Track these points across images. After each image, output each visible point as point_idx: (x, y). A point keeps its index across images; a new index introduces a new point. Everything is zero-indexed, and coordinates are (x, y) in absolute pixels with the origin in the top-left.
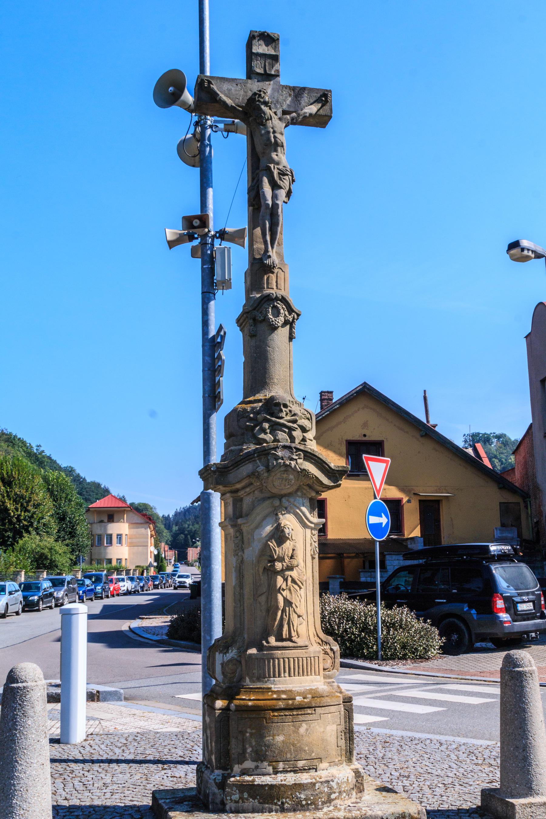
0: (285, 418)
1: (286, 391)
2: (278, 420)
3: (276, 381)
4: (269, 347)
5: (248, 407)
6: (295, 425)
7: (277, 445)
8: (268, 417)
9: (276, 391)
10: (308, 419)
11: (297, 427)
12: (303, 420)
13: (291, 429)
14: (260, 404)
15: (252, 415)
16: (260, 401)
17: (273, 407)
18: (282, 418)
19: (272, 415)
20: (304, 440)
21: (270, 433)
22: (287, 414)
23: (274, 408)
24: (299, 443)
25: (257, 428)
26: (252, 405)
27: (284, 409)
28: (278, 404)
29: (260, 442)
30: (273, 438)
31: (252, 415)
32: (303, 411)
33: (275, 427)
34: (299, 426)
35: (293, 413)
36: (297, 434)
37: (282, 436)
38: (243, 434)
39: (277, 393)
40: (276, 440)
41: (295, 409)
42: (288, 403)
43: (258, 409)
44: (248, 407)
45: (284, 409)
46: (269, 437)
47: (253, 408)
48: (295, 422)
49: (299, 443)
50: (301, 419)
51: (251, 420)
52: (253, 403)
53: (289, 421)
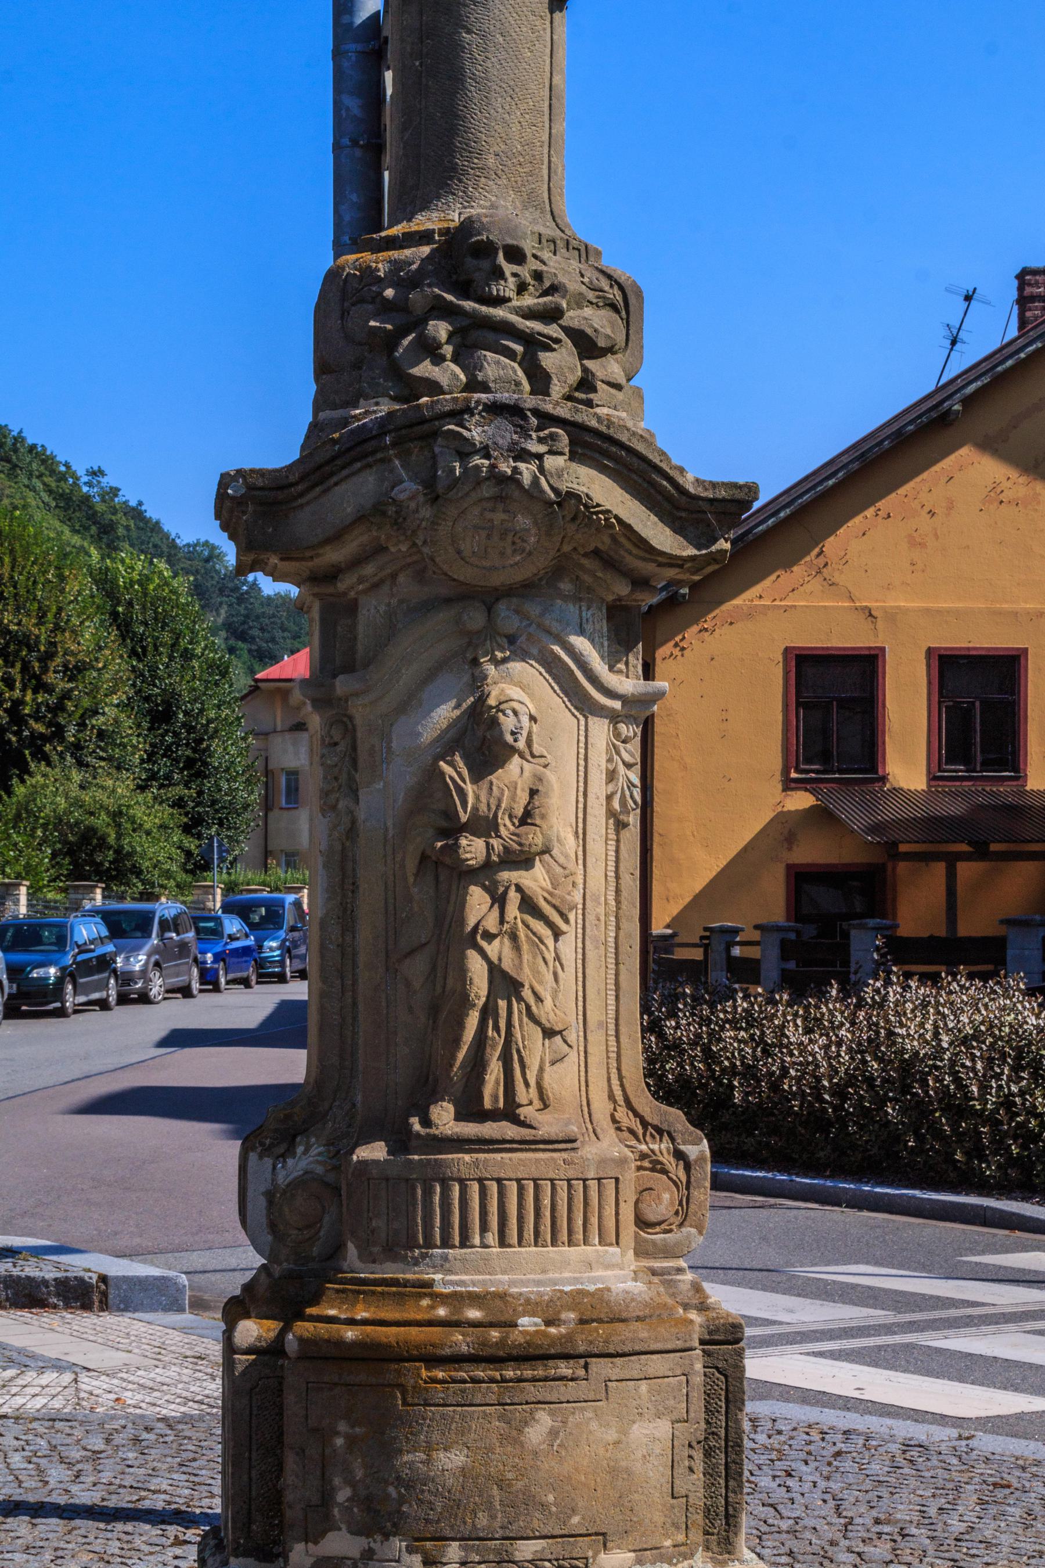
0: (515, 303)
1: (530, 201)
2: (484, 309)
3: (491, 161)
4: (469, 32)
5: (380, 263)
6: (553, 330)
7: (468, 400)
8: (449, 297)
9: (491, 203)
10: (613, 307)
11: (562, 335)
12: (588, 311)
13: (534, 344)
14: (426, 250)
15: (389, 293)
16: (425, 237)
17: (469, 259)
18: (500, 301)
19: (465, 290)
20: (586, 383)
21: (455, 360)
22: (522, 288)
23: (470, 262)
24: (569, 398)
25: (406, 342)
26: (395, 254)
27: (508, 268)
28: (487, 250)
29: (411, 388)
30: (462, 377)
31: (389, 293)
32: (590, 275)
33: (475, 335)
34: (568, 331)
35: (547, 284)
36: (561, 362)
37: (499, 368)
38: (357, 366)
39: (493, 206)
40: (474, 385)
41: (562, 268)
42: (528, 246)
43: (414, 267)
44: (380, 263)
45: (508, 268)
46: (449, 374)
47: (397, 266)
48: (552, 315)
49: (569, 398)
50: (580, 307)
51: (387, 308)
52: (402, 247)
53: (530, 314)
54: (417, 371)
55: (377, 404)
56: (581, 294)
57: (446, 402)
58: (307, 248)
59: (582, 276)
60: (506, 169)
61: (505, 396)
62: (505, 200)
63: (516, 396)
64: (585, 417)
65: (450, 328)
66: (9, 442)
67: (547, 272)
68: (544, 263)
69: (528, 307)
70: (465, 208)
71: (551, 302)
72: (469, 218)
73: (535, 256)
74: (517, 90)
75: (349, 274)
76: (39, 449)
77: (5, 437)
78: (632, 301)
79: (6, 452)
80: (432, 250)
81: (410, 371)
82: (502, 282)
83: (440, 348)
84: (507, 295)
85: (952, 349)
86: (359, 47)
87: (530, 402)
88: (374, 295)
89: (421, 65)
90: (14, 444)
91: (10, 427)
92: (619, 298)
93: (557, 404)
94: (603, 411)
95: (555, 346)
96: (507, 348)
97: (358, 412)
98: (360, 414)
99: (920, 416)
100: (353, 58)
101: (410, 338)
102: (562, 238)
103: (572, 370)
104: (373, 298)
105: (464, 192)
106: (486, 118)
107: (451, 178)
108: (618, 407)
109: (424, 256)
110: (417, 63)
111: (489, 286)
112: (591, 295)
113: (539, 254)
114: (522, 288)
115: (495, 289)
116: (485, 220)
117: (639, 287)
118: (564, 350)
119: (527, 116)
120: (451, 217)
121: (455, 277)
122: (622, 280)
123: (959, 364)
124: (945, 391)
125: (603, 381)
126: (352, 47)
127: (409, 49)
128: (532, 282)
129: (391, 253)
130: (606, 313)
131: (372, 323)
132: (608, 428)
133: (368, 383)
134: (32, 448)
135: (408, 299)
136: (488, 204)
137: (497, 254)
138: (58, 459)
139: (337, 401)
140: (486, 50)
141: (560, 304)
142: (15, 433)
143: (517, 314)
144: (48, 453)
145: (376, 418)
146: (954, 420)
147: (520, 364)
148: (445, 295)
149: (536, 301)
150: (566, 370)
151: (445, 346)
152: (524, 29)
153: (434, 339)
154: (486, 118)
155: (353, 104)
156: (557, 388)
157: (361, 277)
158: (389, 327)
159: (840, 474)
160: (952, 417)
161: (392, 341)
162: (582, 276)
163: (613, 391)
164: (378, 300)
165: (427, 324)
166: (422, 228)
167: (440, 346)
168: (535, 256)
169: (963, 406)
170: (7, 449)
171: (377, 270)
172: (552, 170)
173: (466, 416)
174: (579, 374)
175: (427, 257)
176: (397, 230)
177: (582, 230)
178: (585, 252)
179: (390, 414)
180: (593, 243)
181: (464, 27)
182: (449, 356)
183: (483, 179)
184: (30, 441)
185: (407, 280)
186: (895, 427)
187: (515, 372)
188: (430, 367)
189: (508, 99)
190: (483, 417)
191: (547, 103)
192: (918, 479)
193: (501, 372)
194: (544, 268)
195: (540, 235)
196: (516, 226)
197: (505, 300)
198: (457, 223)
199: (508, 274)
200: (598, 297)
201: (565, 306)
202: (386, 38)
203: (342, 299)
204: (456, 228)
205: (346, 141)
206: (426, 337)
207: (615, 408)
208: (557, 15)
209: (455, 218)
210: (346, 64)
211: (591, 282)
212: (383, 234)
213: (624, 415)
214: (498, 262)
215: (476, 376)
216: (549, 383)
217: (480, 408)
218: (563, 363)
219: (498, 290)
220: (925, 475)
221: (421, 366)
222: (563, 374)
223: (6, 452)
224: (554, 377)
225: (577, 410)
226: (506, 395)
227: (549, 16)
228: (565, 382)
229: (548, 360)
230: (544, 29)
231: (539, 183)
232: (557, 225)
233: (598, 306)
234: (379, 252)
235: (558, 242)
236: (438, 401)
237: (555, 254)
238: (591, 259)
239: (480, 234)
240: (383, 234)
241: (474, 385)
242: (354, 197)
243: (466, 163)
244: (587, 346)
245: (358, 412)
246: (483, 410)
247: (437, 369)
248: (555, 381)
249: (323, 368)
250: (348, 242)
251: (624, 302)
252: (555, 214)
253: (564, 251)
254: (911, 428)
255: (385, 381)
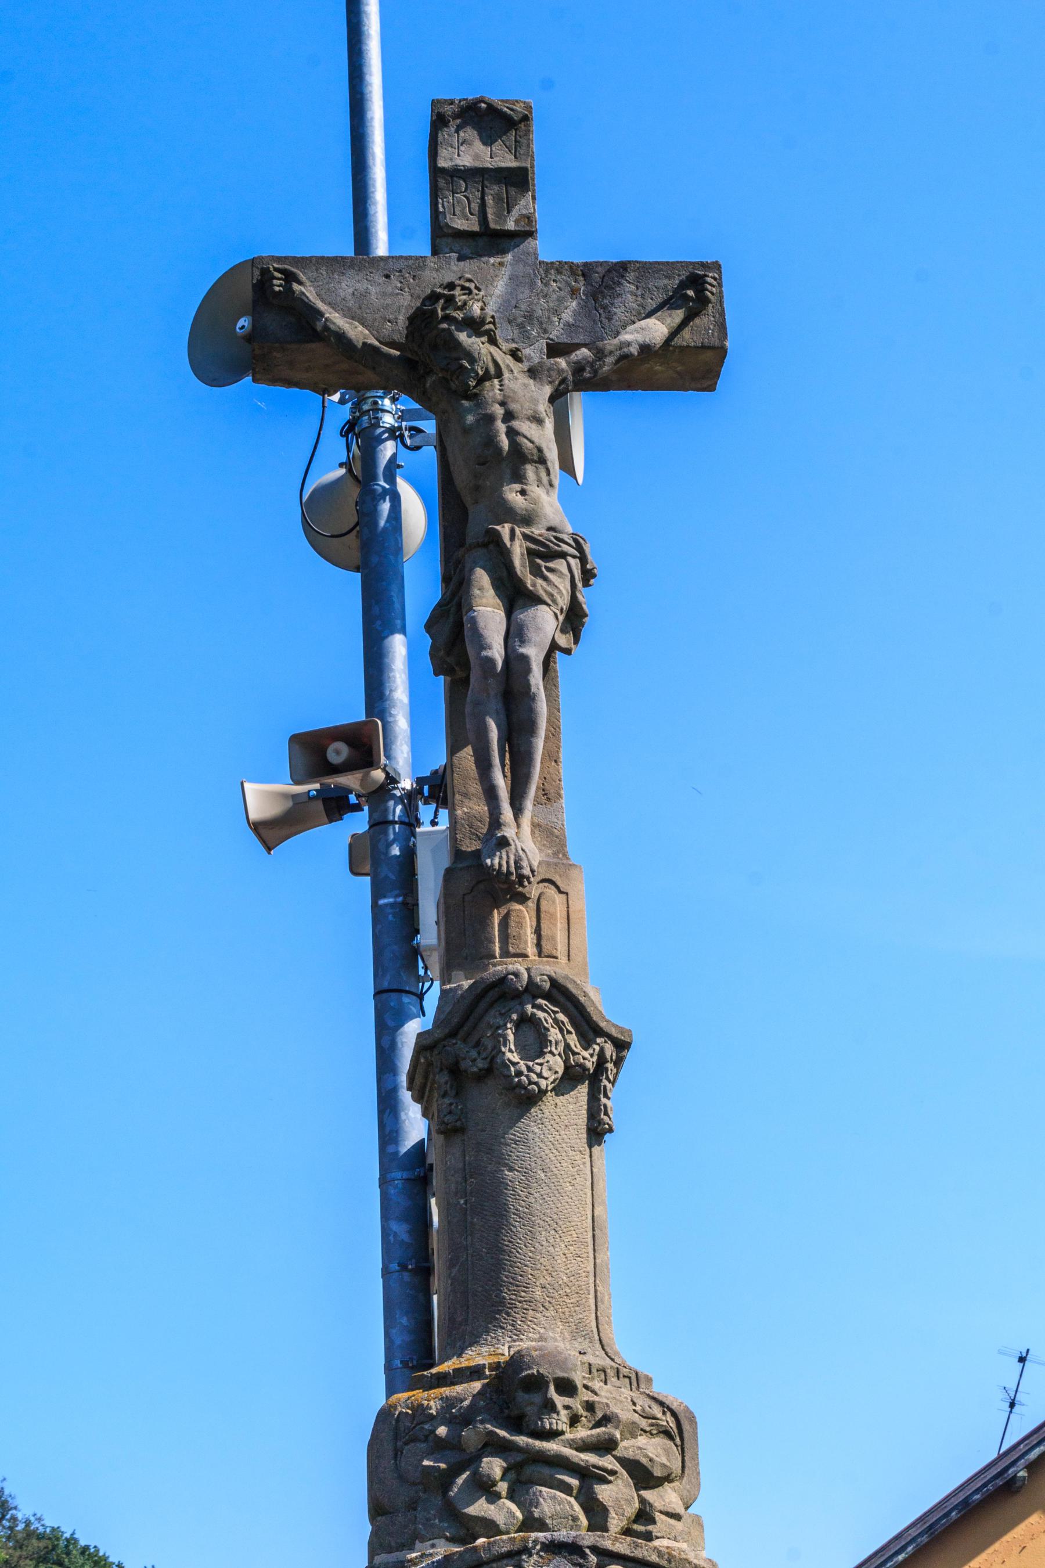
0: (568, 1436)
1: (578, 1331)
2: (538, 1444)
3: (538, 1293)
4: (511, 1169)
5: (432, 1400)
6: (608, 1462)
7: (525, 1540)
8: (502, 1433)
10: (667, 1434)
11: (617, 1467)
12: (642, 1440)
13: (589, 1477)
14: (477, 1386)
15: (442, 1431)
16: (475, 1372)
17: (519, 1394)
18: (553, 1434)
19: (517, 1425)
20: (645, 1515)
21: (511, 1497)
22: (574, 1420)
23: (521, 1396)
24: (627, 1532)
25: (460, 1480)
26: (446, 1391)
27: (560, 1401)
28: (537, 1383)
29: (468, 1529)
30: (519, 1515)
31: (442, 1431)
32: (643, 1402)
33: (529, 1471)
34: (623, 1461)
35: (599, 1415)
36: (617, 1494)
37: (555, 1503)
38: (412, 1506)
39: (541, 1339)
40: (531, 1523)
41: (615, 1398)
42: (579, 1377)
43: (466, 1403)
44: (432, 1400)
45: (560, 1401)
46: (505, 1511)
47: (449, 1403)
48: (606, 1446)
49: (627, 1532)
50: (634, 1436)
51: (440, 1446)
52: (453, 1384)
53: (584, 1447)
54: (472, 1510)
55: (433, 1546)
56: (634, 1423)
57: (503, 1543)
58: (362, 1385)
59: (634, 1404)
60: (553, 1301)
61: (563, 1535)
62: (554, 1332)
63: (573, 1533)
64: (645, 1552)
65: (505, 1465)
66: (62, 1543)
67: (599, 1402)
68: (596, 1394)
69: (582, 1439)
70: (515, 1341)
71: (604, 1433)
72: (519, 1352)
73: (586, 1387)
74: (561, 1223)
75: (401, 1413)
76: (92, 1550)
77: (58, 1539)
78: (686, 1427)
79: (58, 1555)
80: (484, 1386)
81: (466, 1511)
82: (555, 1416)
83: (495, 1485)
84: (560, 1428)
85: (1011, 1412)
86: (405, 1175)
87: (588, 1539)
88: (426, 1433)
89: (466, 1203)
90: (67, 1546)
91: (63, 1529)
92: (673, 1424)
93: (616, 1539)
94: (665, 1543)
95: (611, 1478)
96: (562, 1482)
97: (414, 1555)
98: (416, 1558)
99: (985, 1485)
100: (400, 1186)
101: (464, 1476)
102: (612, 1367)
103: (629, 1502)
104: (427, 1437)
105: (513, 1325)
106: (531, 1251)
107: (499, 1312)
108: (679, 1538)
109: (475, 1392)
110: (462, 1202)
111: (541, 1420)
112: (644, 1423)
113: (590, 1384)
114: (574, 1420)
115: (549, 1422)
116: (535, 1354)
117: (691, 1413)
118: (620, 1482)
119: (571, 1248)
120: (500, 1351)
121: (506, 1411)
122: (674, 1407)
123: (1021, 1427)
124: (1008, 1457)
125: (661, 1512)
126: (398, 1175)
127: (453, 1186)
128: (585, 1414)
129: (442, 1390)
130: (660, 1441)
131: (426, 1463)
132: (670, 1562)
133: (423, 1524)
134: (85, 1549)
135: (460, 1436)
136: (537, 1336)
137: (548, 1387)
138: (111, 1560)
139: (393, 1544)
140: (528, 1186)
141: (614, 1435)
142: (67, 1535)
143: (571, 1447)
144: (101, 1554)
145: (433, 1563)
146: (1021, 1487)
147: (576, 1498)
148: (498, 1431)
149: (589, 1432)
150: (623, 1502)
151: (500, 1484)
152: (565, 1164)
153: (489, 1476)
154: (531, 1251)
155: (402, 1230)
156: (615, 1522)
157: (413, 1416)
158: (443, 1466)
159: (910, 1549)
160: (1018, 1484)
161: (446, 1479)
162: (634, 1404)
163: (672, 1521)
164: (431, 1438)
165: (481, 1462)
166: (472, 1364)
167: (494, 1484)
168: (586, 1387)
169: (1028, 1472)
170: (59, 1551)
171: (429, 1407)
172: (599, 1299)
173: (524, 1557)
174: (637, 1505)
175: (479, 1393)
176: (447, 1366)
177: (632, 1358)
178: (636, 1380)
179: (447, 1558)
180: (643, 1370)
181: (506, 1165)
182: (504, 1494)
183: (531, 1312)
184: (83, 1543)
185: (460, 1418)
186: (961, 1497)
187: (572, 1507)
188: (486, 1505)
189: (553, 1232)
190: (541, 1557)
191: (590, 1234)
192: (990, 1550)
193: (558, 1508)
194: (596, 1398)
195: (590, 1365)
196: (566, 1359)
197: (559, 1433)
198: (507, 1357)
199: (559, 1407)
200: (652, 1425)
201: (618, 1436)
202: (431, 1165)
203: (394, 1439)
204: (507, 1363)
205: (394, 1266)
206: (481, 1475)
207: (675, 1540)
208: (596, 1149)
209: (505, 1352)
210: (392, 1191)
211: (643, 1410)
212: (434, 1371)
213: (684, 1546)
214: (549, 1396)
215: (532, 1513)
216: (607, 1517)
217: (538, 1547)
218: (620, 1495)
219: (550, 1424)
220: (996, 1546)
221: (477, 1505)
222: (620, 1507)
223: (58, 1555)
224: (611, 1510)
225: (637, 1546)
226: (564, 1532)
227: (588, 1150)
228: (623, 1515)
229: (604, 1493)
230: (584, 1163)
231: (587, 1313)
232: (606, 1354)
233: (652, 1434)
234: (431, 1388)
235: (608, 1371)
236: (494, 1541)
237: (606, 1383)
238: (642, 1386)
239: (530, 1368)
240: (434, 1371)
241: (531, 1523)
242: (404, 1321)
243: (514, 1297)
244: (643, 1476)
245: (414, 1555)
246: (541, 1550)
247: (492, 1507)
248: (612, 1514)
249: (377, 1510)
250: (400, 1365)
251: (677, 1428)
252: (604, 1342)
253: (614, 1379)
254: (977, 1497)
255: (440, 1521)
